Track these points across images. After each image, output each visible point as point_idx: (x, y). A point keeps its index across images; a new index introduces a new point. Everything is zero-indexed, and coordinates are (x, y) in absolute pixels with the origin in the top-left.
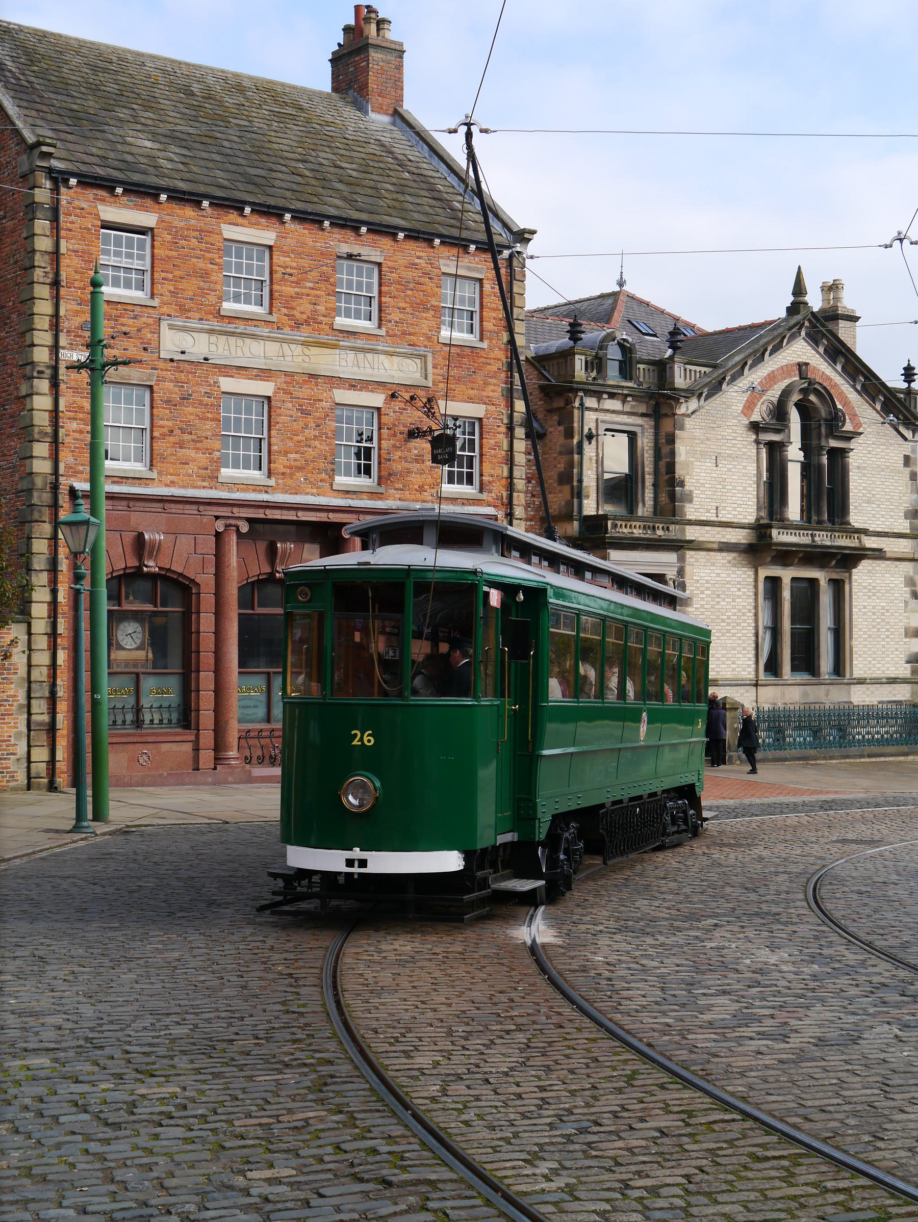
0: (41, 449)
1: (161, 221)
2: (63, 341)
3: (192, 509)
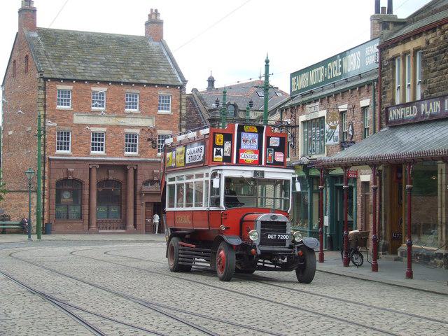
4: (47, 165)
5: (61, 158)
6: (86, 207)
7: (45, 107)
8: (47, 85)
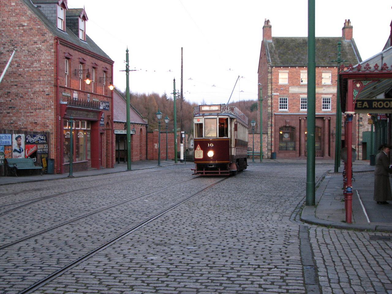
0: (270, 108)
1: (289, 71)
2: (273, 92)
3: (295, 116)
4: (273, 118)
5: (281, 114)
6: (298, 143)
7: (272, 83)
8: (273, 70)
